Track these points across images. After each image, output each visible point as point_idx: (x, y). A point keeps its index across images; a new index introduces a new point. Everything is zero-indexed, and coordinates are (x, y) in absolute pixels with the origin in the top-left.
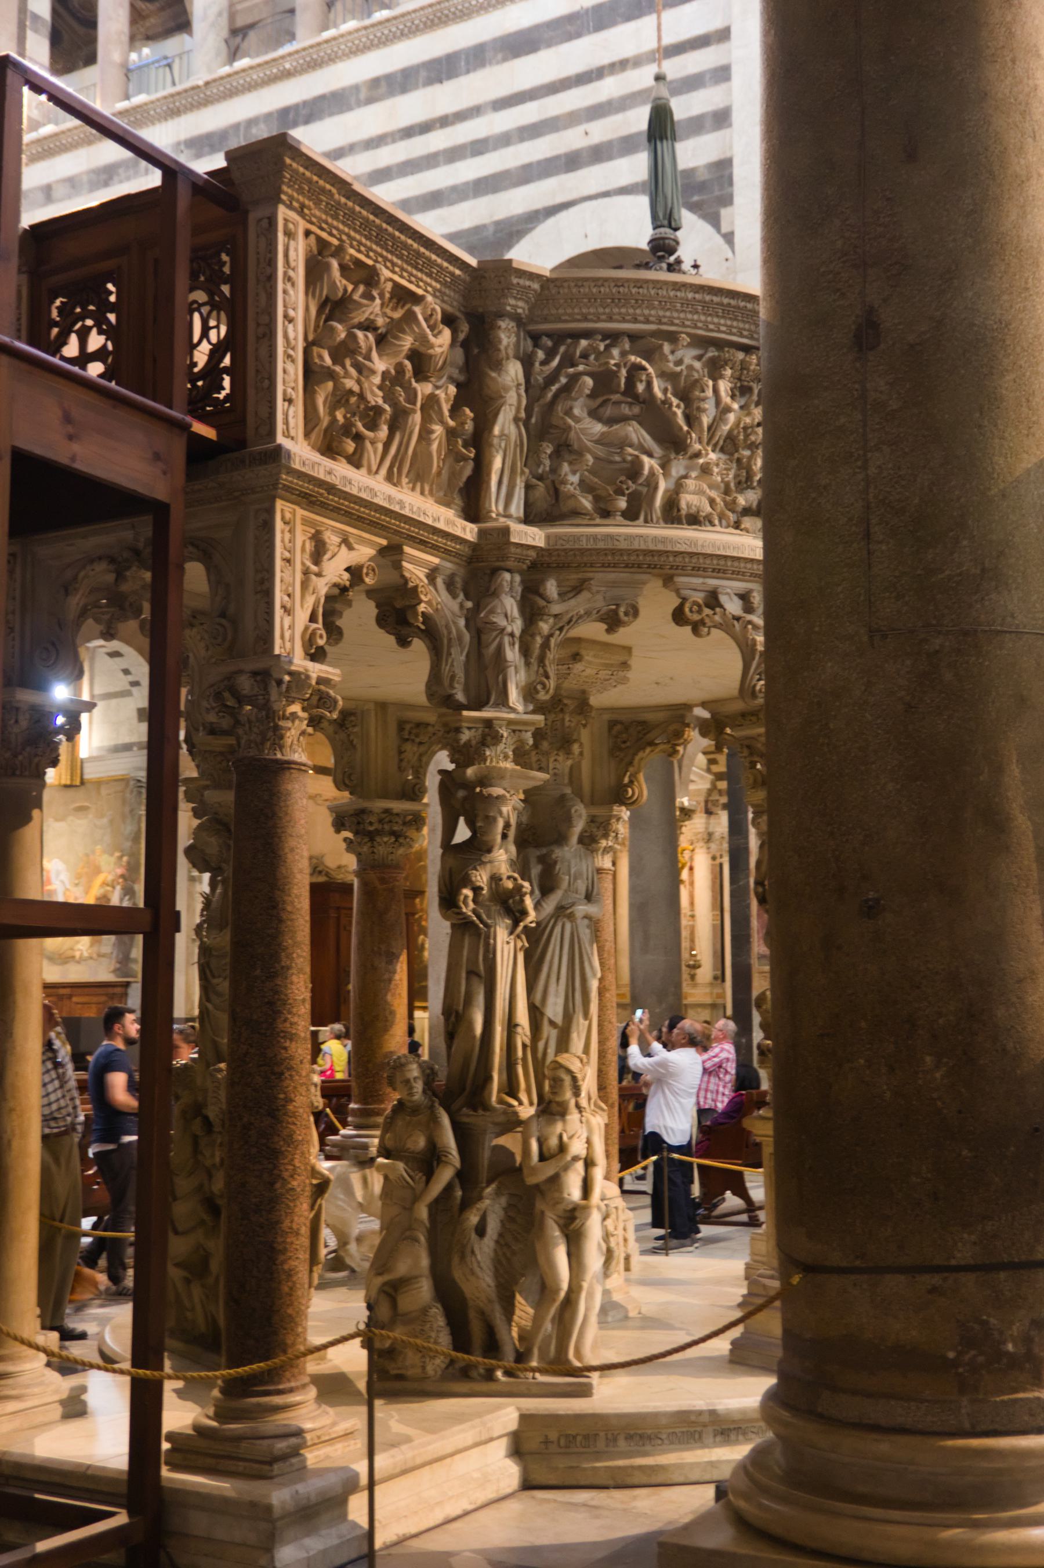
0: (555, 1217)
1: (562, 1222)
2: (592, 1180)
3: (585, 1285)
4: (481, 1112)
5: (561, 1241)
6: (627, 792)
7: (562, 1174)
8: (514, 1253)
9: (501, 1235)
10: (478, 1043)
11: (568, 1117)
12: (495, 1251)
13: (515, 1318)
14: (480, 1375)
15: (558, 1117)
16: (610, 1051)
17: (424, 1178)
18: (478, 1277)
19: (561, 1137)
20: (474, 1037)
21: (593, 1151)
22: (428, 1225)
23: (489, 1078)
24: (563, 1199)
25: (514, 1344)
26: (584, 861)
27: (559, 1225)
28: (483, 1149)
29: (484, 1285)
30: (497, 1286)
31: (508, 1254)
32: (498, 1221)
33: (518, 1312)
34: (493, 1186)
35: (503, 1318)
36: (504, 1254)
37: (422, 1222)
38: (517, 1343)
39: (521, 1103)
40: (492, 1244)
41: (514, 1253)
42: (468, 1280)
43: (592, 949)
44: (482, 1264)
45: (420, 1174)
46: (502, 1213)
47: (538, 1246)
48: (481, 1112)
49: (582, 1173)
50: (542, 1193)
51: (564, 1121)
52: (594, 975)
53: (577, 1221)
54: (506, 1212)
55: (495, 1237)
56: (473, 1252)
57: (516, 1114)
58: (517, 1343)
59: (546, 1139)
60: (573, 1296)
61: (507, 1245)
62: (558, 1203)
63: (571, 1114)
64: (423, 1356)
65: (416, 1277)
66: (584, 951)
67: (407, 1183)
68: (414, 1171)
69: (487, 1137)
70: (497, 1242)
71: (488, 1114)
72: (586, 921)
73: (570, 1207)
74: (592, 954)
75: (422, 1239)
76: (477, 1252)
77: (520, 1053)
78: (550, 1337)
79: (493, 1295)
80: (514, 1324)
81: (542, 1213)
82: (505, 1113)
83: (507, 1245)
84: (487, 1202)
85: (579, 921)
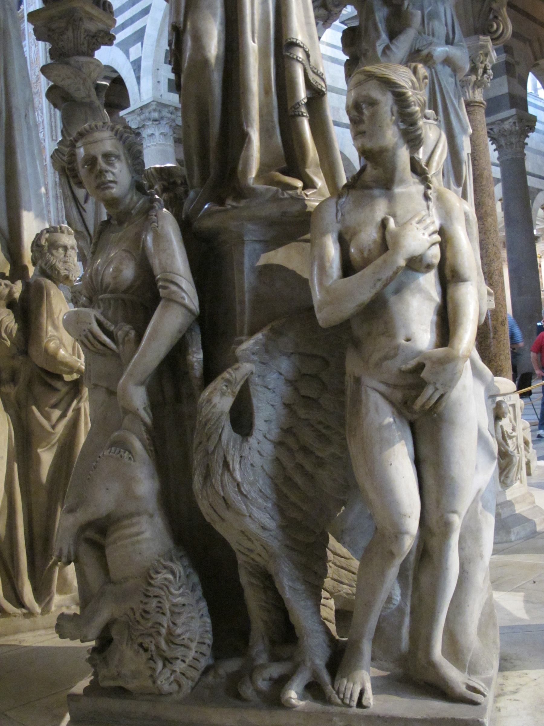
0: (383, 388)
1: (398, 395)
2: (457, 307)
3: (457, 521)
4: (230, 203)
5: (397, 434)
6: (492, 26)
7: (392, 299)
8: (320, 463)
9: (287, 431)
10: (216, 77)
11: (398, 190)
12: (277, 460)
13: (328, 582)
14: (259, 692)
15: (376, 192)
16: (497, 272)
17: (133, 333)
18: (239, 513)
19: (384, 224)
20: (205, 62)
21: (455, 255)
22: (148, 420)
23: (244, 137)
24: (397, 347)
25: (328, 631)
26: (440, 4)
27: (392, 403)
28: (242, 272)
29: (253, 527)
30: (283, 528)
31: (309, 467)
32: (278, 403)
33: (331, 570)
34: (259, 336)
35: (300, 587)
36: (300, 467)
37: (135, 414)
38: (333, 627)
39: (309, 184)
40: (268, 448)
41: (320, 463)
42: (223, 520)
43: (459, 102)
44: (245, 488)
45: (127, 327)
46: (283, 389)
47: (353, 448)
48: (230, 203)
49: (437, 298)
50: (357, 344)
51: (391, 198)
52: (464, 131)
53: (429, 391)
54: (296, 389)
55: (274, 433)
56: (226, 465)
57: (300, 200)
58: (333, 627)
59: (355, 233)
60: (434, 542)
61: (306, 450)
62: (386, 358)
63: (402, 182)
64: (151, 659)
65: (131, 516)
66: (448, 101)
67: (104, 344)
68: (116, 323)
69: (248, 249)
70: (279, 444)
71: (243, 203)
72: (448, 70)
73: (412, 363)
74: (462, 110)
75: (138, 445)
76: (235, 466)
77: (302, 94)
78: (400, 610)
79: (275, 544)
80: (324, 594)
81: (358, 381)
82: (275, 198)
83: (306, 450)
84: (246, 367)
85: (439, 67)
